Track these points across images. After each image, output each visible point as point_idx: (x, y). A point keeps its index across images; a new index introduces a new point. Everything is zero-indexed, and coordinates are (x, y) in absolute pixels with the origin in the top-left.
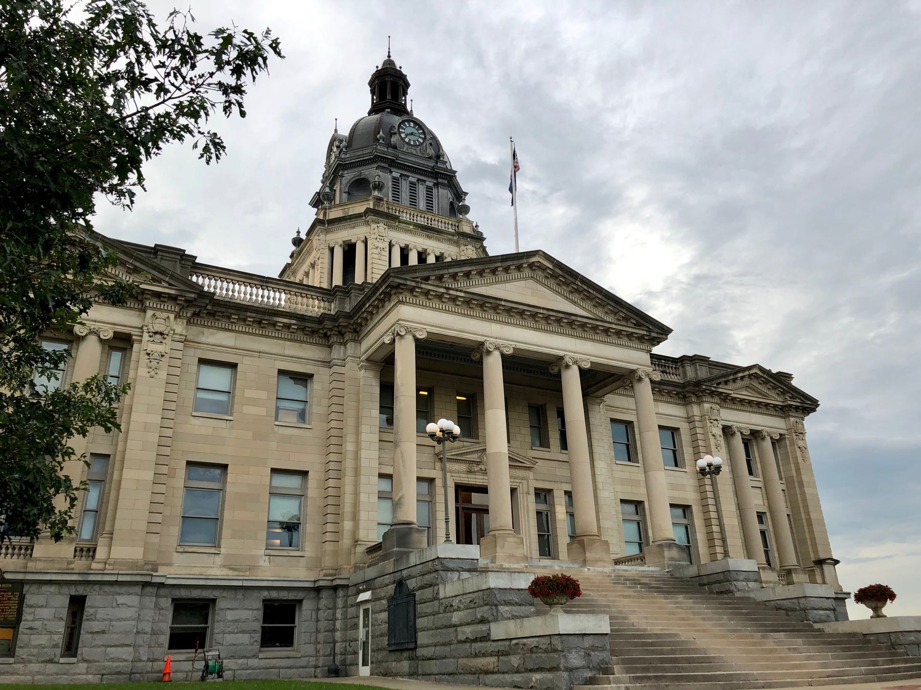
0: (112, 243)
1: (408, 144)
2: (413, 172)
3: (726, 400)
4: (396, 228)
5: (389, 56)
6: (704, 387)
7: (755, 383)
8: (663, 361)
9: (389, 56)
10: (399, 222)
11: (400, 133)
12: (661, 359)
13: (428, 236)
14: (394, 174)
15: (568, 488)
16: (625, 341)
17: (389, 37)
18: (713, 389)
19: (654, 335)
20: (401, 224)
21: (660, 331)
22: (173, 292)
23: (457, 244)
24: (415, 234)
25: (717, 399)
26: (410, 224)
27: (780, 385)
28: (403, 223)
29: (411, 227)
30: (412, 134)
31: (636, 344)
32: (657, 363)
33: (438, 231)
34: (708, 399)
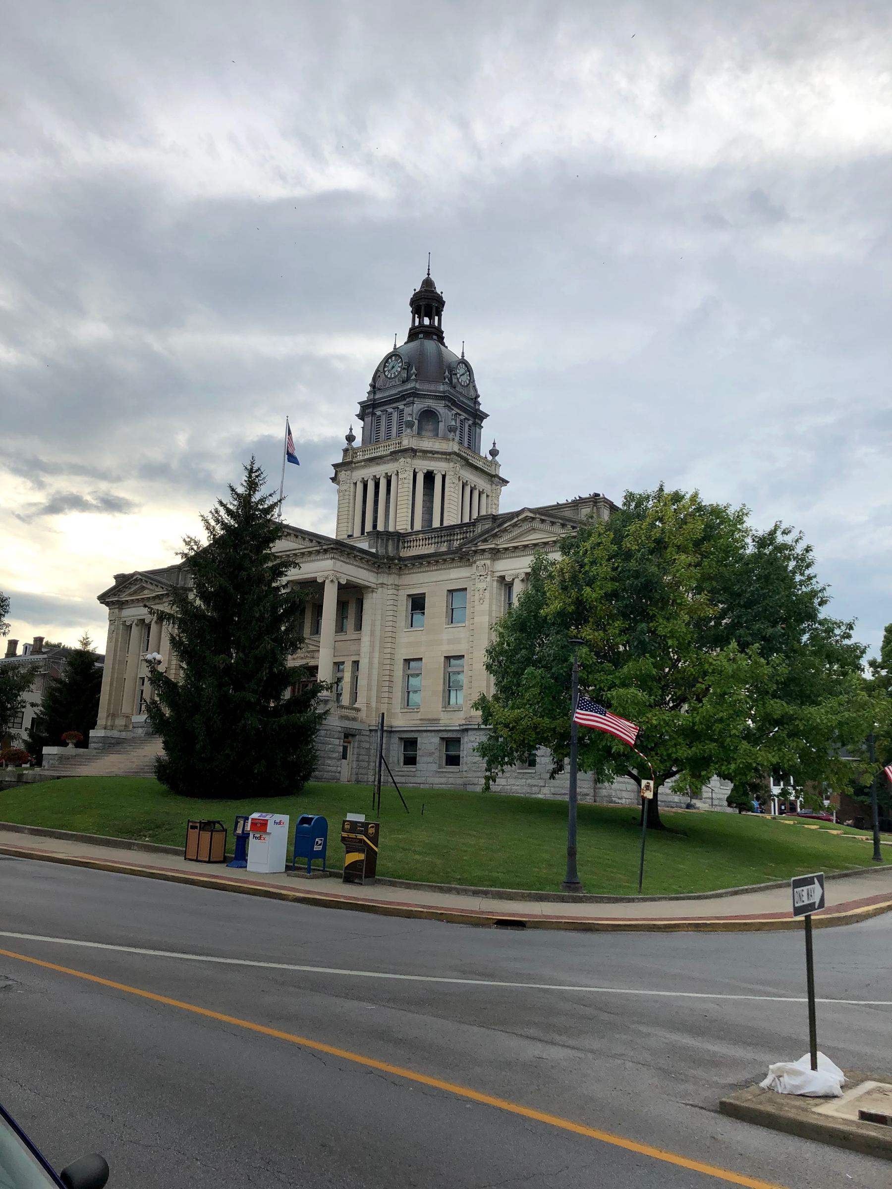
0: (152, 576)
1: (390, 378)
2: (386, 405)
3: (496, 554)
4: (356, 468)
5: (429, 274)
6: (464, 550)
7: (537, 524)
8: (465, 528)
9: (429, 274)
10: (355, 464)
11: (384, 372)
12: (463, 527)
13: (377, 464)
14: (379, 413)
15: (355, 658)
16: (313, 557)
17: (429, 253)
18: (473, 549)
19: (325, 547)
20: (357, 465)
21: (329, 543)
22: (165, 592)
23: (396, 460)
24: (369, 466)
25: (487, 555)
26: (361, 462)
27: (557, 521)
28: (358, 463)
29: (363, 463)
30: (393, 367)
31: (321, 556)
32: (468, 530)
33: (381, 457)
34: (478, 557)
